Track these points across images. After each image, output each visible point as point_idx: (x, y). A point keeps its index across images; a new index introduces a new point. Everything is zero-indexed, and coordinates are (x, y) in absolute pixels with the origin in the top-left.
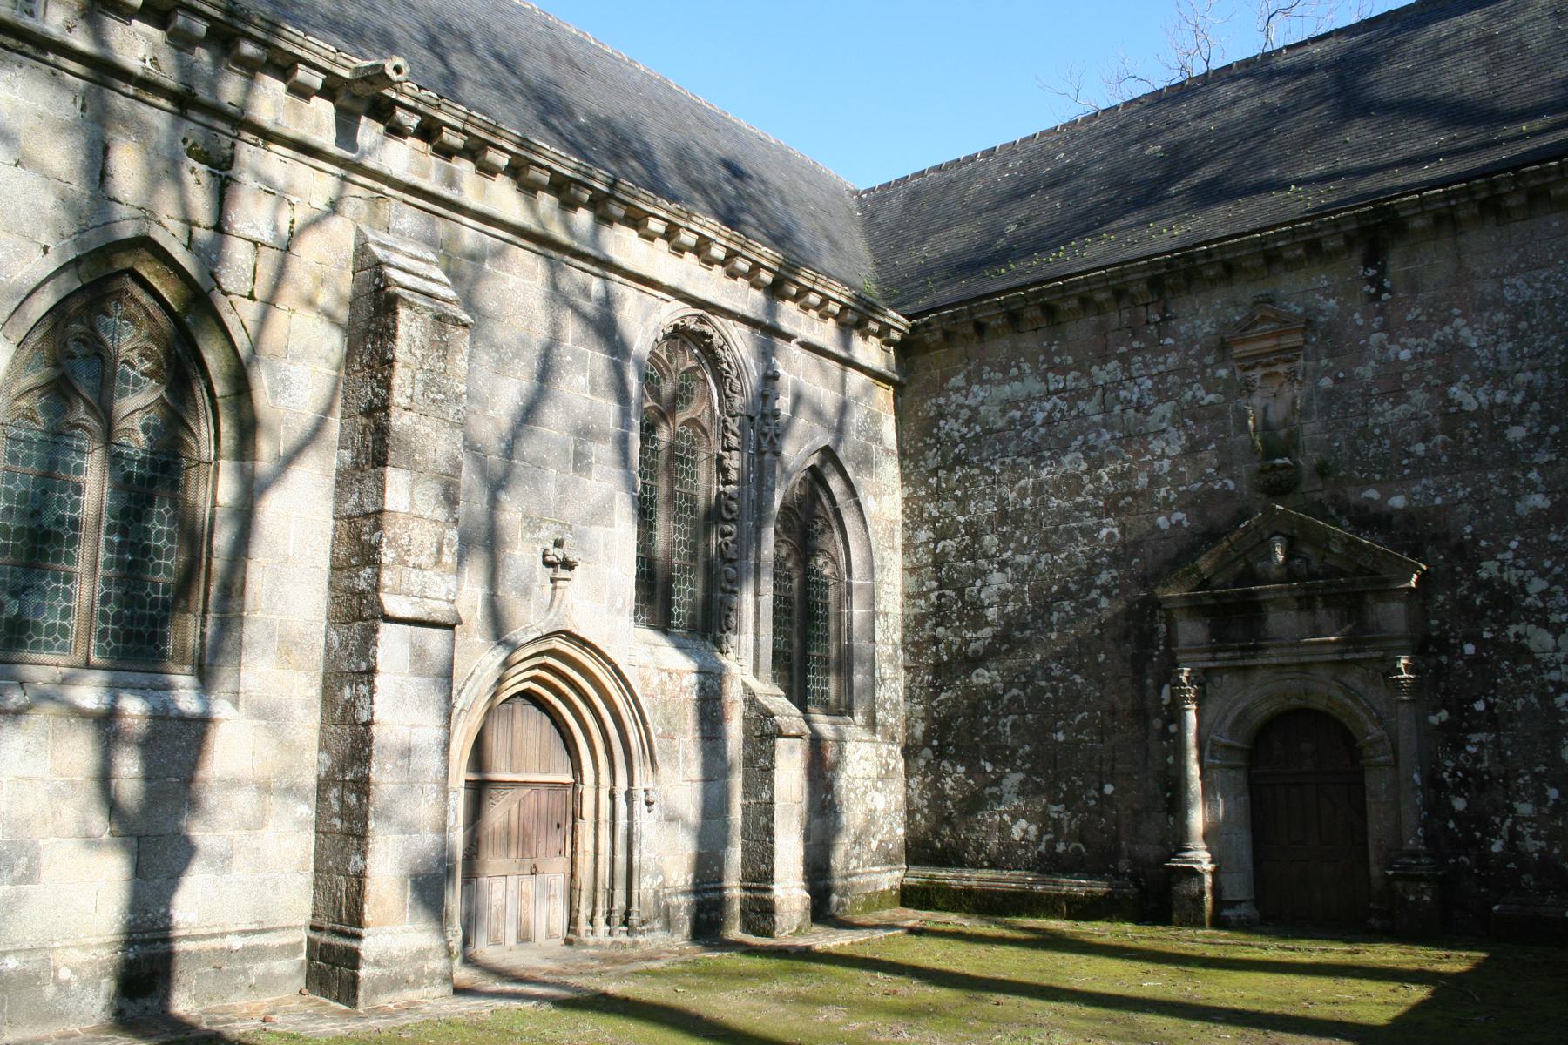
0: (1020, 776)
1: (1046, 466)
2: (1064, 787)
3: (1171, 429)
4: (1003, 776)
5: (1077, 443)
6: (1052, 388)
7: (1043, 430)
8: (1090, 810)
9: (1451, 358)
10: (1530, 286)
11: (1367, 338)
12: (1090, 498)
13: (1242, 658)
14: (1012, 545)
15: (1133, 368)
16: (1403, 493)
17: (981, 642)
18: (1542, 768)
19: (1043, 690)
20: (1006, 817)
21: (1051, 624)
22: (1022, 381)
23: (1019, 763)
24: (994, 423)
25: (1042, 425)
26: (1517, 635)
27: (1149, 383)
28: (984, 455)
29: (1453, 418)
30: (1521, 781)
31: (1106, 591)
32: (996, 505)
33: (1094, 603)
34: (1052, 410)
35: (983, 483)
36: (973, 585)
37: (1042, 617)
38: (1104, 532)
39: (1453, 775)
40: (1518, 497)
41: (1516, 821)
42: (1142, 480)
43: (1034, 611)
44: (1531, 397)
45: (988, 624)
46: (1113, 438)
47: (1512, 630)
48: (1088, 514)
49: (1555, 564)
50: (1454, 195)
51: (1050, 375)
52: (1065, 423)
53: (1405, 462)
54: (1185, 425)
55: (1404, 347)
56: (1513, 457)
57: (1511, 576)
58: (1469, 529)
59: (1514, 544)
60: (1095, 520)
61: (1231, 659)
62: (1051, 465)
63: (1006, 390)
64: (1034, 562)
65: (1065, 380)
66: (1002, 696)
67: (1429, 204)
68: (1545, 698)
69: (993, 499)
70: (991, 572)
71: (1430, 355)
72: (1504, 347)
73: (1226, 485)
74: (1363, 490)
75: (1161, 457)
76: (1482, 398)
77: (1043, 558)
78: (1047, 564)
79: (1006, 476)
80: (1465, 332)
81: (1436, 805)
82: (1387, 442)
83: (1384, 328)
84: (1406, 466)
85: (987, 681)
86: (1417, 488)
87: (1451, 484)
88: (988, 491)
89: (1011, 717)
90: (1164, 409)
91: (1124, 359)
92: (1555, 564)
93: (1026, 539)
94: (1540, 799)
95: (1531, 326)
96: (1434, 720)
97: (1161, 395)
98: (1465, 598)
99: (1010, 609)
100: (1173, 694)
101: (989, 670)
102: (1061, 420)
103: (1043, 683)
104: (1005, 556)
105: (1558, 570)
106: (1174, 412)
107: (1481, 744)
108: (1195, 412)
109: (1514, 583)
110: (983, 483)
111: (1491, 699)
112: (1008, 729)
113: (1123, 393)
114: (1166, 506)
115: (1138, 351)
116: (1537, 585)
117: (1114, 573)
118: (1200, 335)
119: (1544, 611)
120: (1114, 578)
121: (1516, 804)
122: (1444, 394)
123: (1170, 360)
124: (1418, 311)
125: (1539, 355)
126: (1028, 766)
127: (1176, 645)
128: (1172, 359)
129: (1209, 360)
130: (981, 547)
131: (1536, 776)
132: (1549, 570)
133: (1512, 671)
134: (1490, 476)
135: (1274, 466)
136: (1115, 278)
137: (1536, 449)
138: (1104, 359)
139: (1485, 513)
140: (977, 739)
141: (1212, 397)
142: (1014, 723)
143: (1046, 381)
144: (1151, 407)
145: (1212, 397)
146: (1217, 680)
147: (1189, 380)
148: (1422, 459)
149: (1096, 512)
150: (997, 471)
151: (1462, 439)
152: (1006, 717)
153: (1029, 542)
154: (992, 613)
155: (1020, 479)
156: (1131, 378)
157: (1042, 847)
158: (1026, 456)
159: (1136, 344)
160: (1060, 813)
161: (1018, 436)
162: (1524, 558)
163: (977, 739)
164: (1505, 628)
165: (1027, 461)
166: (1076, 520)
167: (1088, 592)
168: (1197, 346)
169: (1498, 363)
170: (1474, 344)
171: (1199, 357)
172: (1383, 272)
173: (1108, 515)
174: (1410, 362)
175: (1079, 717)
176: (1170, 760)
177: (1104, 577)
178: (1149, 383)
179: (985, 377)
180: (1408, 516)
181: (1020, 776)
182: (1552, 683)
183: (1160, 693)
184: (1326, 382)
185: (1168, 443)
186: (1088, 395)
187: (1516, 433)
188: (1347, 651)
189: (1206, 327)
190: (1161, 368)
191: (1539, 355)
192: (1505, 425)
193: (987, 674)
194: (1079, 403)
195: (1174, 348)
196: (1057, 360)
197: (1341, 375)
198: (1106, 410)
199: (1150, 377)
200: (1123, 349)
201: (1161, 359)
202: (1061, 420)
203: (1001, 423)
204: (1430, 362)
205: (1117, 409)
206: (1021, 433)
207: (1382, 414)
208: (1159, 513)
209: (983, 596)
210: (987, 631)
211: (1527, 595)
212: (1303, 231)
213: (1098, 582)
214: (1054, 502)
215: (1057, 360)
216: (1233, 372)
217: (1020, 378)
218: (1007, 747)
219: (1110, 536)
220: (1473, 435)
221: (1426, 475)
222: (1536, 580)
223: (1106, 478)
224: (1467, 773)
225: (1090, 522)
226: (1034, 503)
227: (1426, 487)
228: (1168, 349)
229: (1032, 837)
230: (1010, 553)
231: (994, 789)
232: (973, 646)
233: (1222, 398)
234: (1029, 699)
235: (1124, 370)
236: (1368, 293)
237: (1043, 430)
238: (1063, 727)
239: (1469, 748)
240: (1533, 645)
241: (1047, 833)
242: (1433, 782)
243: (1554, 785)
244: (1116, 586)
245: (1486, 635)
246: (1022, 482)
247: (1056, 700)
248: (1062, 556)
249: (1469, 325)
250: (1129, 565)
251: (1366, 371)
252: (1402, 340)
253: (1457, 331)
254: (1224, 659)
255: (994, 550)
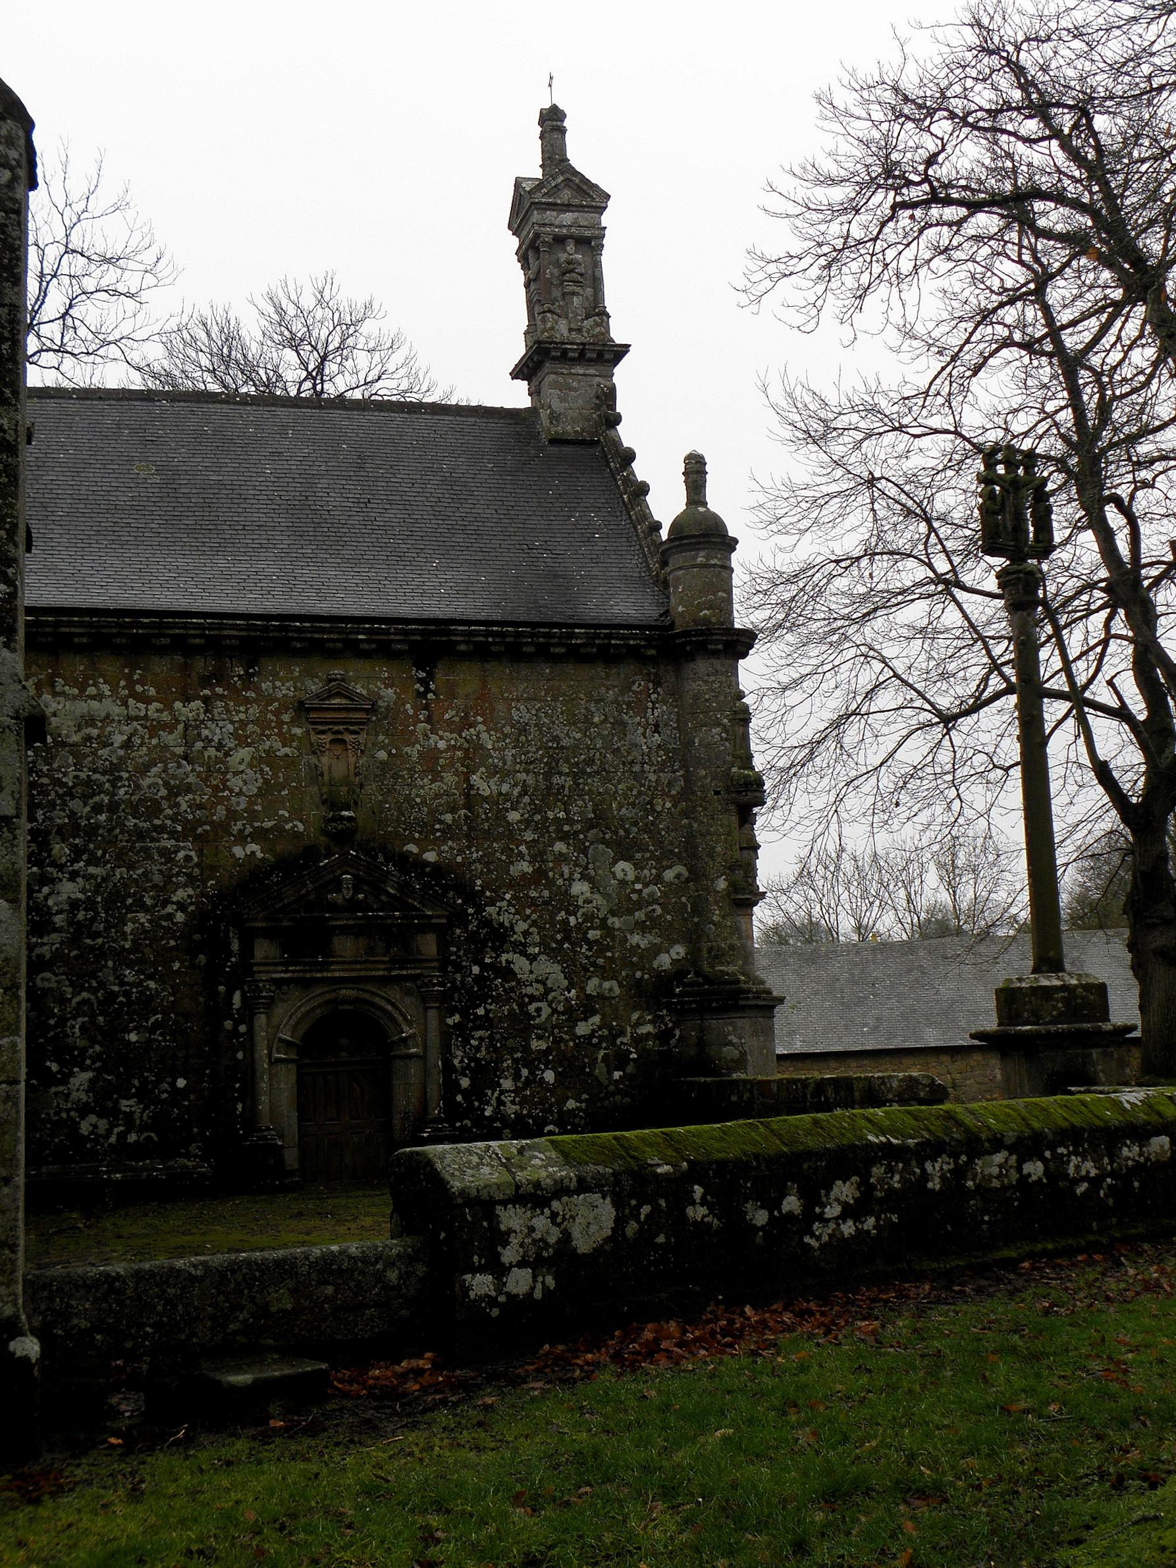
0: (90, 1074)
1: (124, 786)
2: (136, 1082)
3: (249, 771)
4: (72, 1074)
5: (154, 770)
6: (133, 713)
7: (121, 752)
8: (164, 1101)
9: (472, 755)
10: (528, 711)
11: (415, 726)
12: (168, 822)
13: (311, 971)
14: (85, 857)
15: (215, 711)
16: (433, 850)
17: (47, 948)
18: (519, 1055)
19: (114, 995)
20: (73, 1114)
21: (124, 933)
22: (100, 701)
23: (88, 1062)
24: (68, 736)
25: (121, 748)
26: (507, 961)
27: (230, 728)
28: (55, 765)
29: (470, 798)
30: (505, 1065)
31: (181, 907)
32: (68, 817)
33: (170, 917)
34: (132, 735)
35: (53, 793)
36: (39, 891)
37: (115, 926)
38: (181, 855)
39: (462, 1061)
40: (512, 863)
41: (502, 1092)
42: (221, 812)
43: (107, 921)
44: (524, 793)
45: (56, 930)
46: (193, 770)
47: (504, 957)
48: (165, 836)
49: (533, 912)
50: (492, 634)
51: (131, 701)
52: (145, 749)
53: (437, 827)
54: (262, 770)
55: (441, 738)
56: (510, 834)
57: (505, 919)
58: (479, 882)
59: (508, 896)
60: (173, 842)
61: (300, 971)
62: (129, 786)
63: (81, 707)
64: (108, 874)
65: (147, 709)
66: (70, 1000)
67: (475, 636)
68: (522, 1006)
69: (64, 810)
70: (61, 880)
71: (460, 748)
72: (509, 754)
73: (296, 826)
74: (405, 845)
75: (240, 793)
76: (494, 787)
77: (118, 872)
78: (122, 878)
79: (79, 790)
80: (484, 736)
81: (451, 1087)
82: (425, 809)
83: (428, 720)
84: (438, 830)
85: (54, 985)
86: (446, 848)
87: (469, 848)
88: (58, 802)
89: (80, 1020)
90: (244, 753)
91: (206, 700)
92: (533, 912)
93: (100, 853)
94: (517, 1077)
95: (527, 741)
96: (450, 1021)
97: (242, 742)
98: (473, 932)
99: (81, 916)
100: (244, 998)
101: (56, 975)
102: (141, 745)
103: (116, 988)
104: (76, 866)
105: (534, 916)
106: (253, 757)
107: (481, 1039)
108: (270, 758)
109: (507, 924)
110: (53, 793)
111: (488, 1007)
112: (77, 1031)
113: (205, 732)
114: (242, 839)
115: (221, 697)
116: (522, 926)
117: (190, 891)
118: (279, 695)
119: (524, 945)
120: (190, 896)
121: (502, 1081)
122: (467, 780)
123: (250, 711)
124: (454, 713)
125: (532, 762)
126: (98, 1064)
127: (253, 957)
128: (254, 710)
129: (286, 718)
130: (50, 856)
131: (515, 1061)
132: (529, 917)
133: (503, 986)
134: (495, 845)
135: (343, 818)
136: (209, 629)
137: (525, 830)
138: (187, 700)
139: (490, 871)
140: (41, 1040)
141: (287, 750)
142: (83, 1023)
143: (127, 707)
144: (230, 749)
145: (287, 750)
146: (285, 988)
147: (267, 732)
148: (449, 826)
149: (173, 834)
150: (71, 784)
151: (478, 816)
152: (74, 1018)
153: (103, 855)
154: (59, 920)
155: (94, 795)
156: (212, 720)
157: (113, 1139)
158: (104, 773)
159: (219, 690)
160: (131, 1106)
161: (94, 754)
162: (514, 906)
163: (41, 1040)
164: (498, 956)
165: (104, 779)
166: (153, 840)
167: (164, 906)
168: (276, 704)
169: (505, 763)
170: (490, 747)
171: (277, 713)
172: (431, 676)
173: (185, 839)
174: (445, 751)
175: (152, 1020)
176: (240, 1055)
177: (180, 895)
178: (230, 728)
179: (58, 689)
180: (438, 870)
181: (90, 1074)
182: (526, 995)
183: (231, 999)
184: (382, 755)
185: (245, 783)
186: (170, 728)
187: (514, 816)
188: (395, 969)
189: (286, 690)
190: (242, 716)
191: (532, 762)
192: (507, 810)
193: (54, 978)
194: (161, 733)
195: (256, 701)
196: (139, 688)
197: (394, 751)
198: (189, 745)
199: (232, 722)
200: (207, 692)
201: (242, 709)
202: (141, 745)
203: (76, 738)
204: (459, 754)
205: (199, 745)
206: (97, 751)
207: (422, 787)
208: (235, 844)
209: (50, 902)
210: (55, 937)
211: (515, 933)
212: (380, 632)
213: (174, 899)
214: (131, 822)
215: (139, 688)
216: (308, 732)
217: (99, 697)
218: (77, 1048)
219: (188, 858)
220: (486, 814)
221: (451, 838)
222: (520, 922)
223: (184, 806)
224: (470, 1060)
225: (169, 844)
226: (109, 820)
227: (451, 848)
228: (247, 701)
229: (101, 1131)
230: (82, 864)
231: (61, 1088)
232: (38, 951)
233: (296, 753)
234: (99, 1002)
235: (206, 712)
236: (418, 691)
237: (121, 752)
238: (135, 1028)
239: (472, 1042)
240: (516, 968)
241: (118, 1126)
242: (448, 1068)
243: (525, 1066)
244: (191, 904)
245: (487, 960)
246: (97, 799)
247: (129, 1003)
248: (139, 872)
249: (487, 731)
250: (204, 883)
251: (413, 752)
252: (440, 733)
253: (478, 736)
254: (292, 971)
255: (64, 860)
